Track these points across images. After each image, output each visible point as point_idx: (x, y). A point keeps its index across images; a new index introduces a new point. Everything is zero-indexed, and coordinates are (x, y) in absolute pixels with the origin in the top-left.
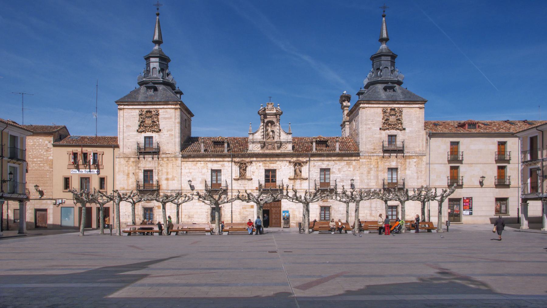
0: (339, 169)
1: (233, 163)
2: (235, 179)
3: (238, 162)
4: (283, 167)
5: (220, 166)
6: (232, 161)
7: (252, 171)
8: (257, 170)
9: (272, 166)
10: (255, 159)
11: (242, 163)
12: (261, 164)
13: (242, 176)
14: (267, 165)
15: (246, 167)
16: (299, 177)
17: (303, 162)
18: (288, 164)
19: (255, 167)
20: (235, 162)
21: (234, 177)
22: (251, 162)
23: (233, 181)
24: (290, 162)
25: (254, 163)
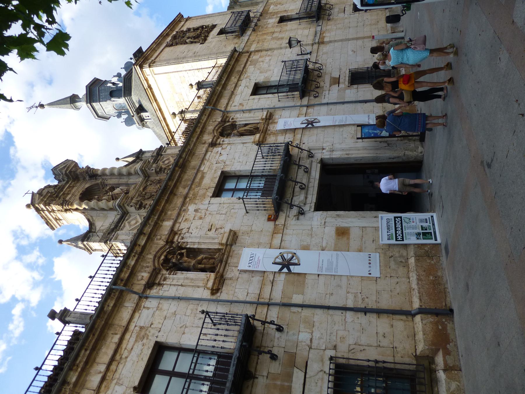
0: (260, 72)
1: (154, 292)
2: (215, 291)
3: (155, 273)
5: (138, 347)
6: (142, 296)
8: (208, 219)
9: (210, 180)
10: (167, 224)
13: (213, 262)
14: (201, 192)
20: (150, 285)
21: (206, 294)
23: (224, 295)
24: (213, 144)
25: (183, 226)
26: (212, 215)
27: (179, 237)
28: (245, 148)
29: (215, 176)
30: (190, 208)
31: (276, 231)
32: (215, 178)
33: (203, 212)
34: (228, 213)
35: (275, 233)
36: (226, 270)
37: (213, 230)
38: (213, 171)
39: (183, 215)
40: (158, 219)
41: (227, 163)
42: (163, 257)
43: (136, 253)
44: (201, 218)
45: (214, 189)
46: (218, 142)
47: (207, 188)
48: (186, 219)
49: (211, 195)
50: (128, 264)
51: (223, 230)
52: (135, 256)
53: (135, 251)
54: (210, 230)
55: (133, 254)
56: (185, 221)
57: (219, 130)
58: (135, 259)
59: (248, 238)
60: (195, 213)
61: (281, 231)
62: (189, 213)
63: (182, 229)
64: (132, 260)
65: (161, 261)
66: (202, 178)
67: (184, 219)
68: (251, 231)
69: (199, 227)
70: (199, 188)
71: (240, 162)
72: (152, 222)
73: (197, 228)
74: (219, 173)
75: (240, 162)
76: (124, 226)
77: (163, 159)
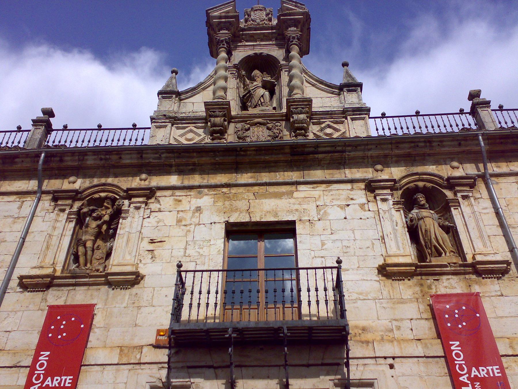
4: (335, 213)
7: (149, 233)
8: (178, 231)
9: (268, 208)
10: (174, 180)
11: (99, 203)
12: (206, 200)
14: (242, 204)
15: (117, 214)
16: (448, 258)
17: (452, 183)
18: (360, 195)
19: (170, 218)
20: (57, 196)
22: (150, 193)
24: (371, 187)
25: (166, 200)
26: (186, 236)
27: (139, 202)
28: (369, 244)
29: (280, 214)
30: (206, 198)
31: (126, 351)
32: (276, 215)
33: (194, 220)
34: (188, 259)
35: (121, 351)
36: (63, 288)
37: (151, 247)
38: (297, 207)
39: (189, 193)
40: (178, 165)
41: (319, 225)
42: (103, 195)
43: (106, 159)
44: (179, 221)
45: (247, 220)
46: (377, 192)
47: (251, 210)
48: (180, 201)
49: (232, 220)
50: (86, 157)
51: (149, 261)
52: (101, 159)
53: (108, 157)
54: (152, 241)
55: (103, 157)
56: (176, 200)
57: (421, 184)
58: (98, 162)
59: (124, 305)
60: (193, 208)
61: (124, 361)
62: (194, 201)
63: (159, 202)
64: (95, 159)
65: (96, 196)
66: (278, 196)
67: (180, 198)
68: (139, 308)
69: (161, 224)
70: (252, 197)
71: (323, 244)
72: (167, 158)
73: (158, 222)
74: (290, 218)
75: (323, 244)
76: (184, 128)
77: (337, 123)
